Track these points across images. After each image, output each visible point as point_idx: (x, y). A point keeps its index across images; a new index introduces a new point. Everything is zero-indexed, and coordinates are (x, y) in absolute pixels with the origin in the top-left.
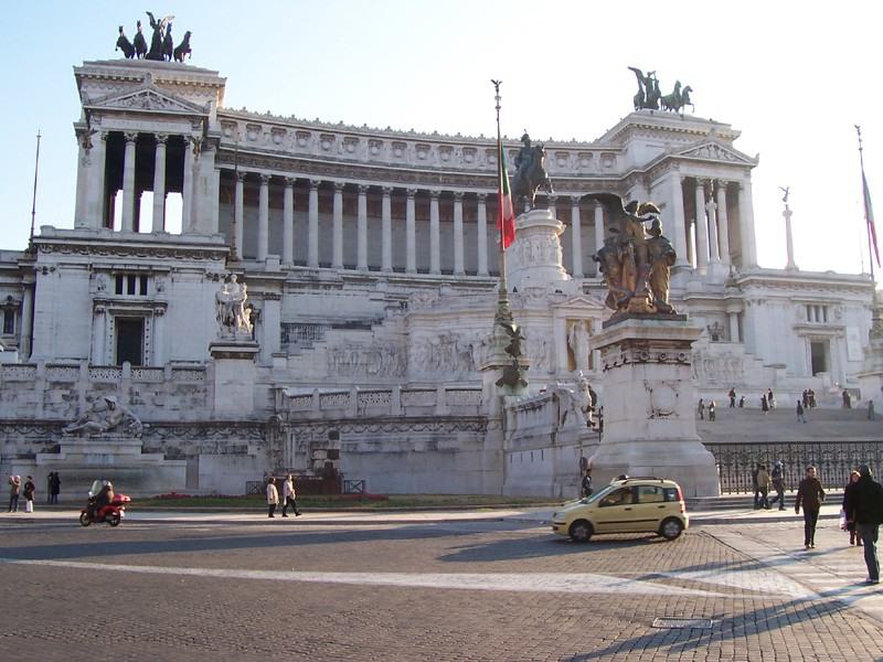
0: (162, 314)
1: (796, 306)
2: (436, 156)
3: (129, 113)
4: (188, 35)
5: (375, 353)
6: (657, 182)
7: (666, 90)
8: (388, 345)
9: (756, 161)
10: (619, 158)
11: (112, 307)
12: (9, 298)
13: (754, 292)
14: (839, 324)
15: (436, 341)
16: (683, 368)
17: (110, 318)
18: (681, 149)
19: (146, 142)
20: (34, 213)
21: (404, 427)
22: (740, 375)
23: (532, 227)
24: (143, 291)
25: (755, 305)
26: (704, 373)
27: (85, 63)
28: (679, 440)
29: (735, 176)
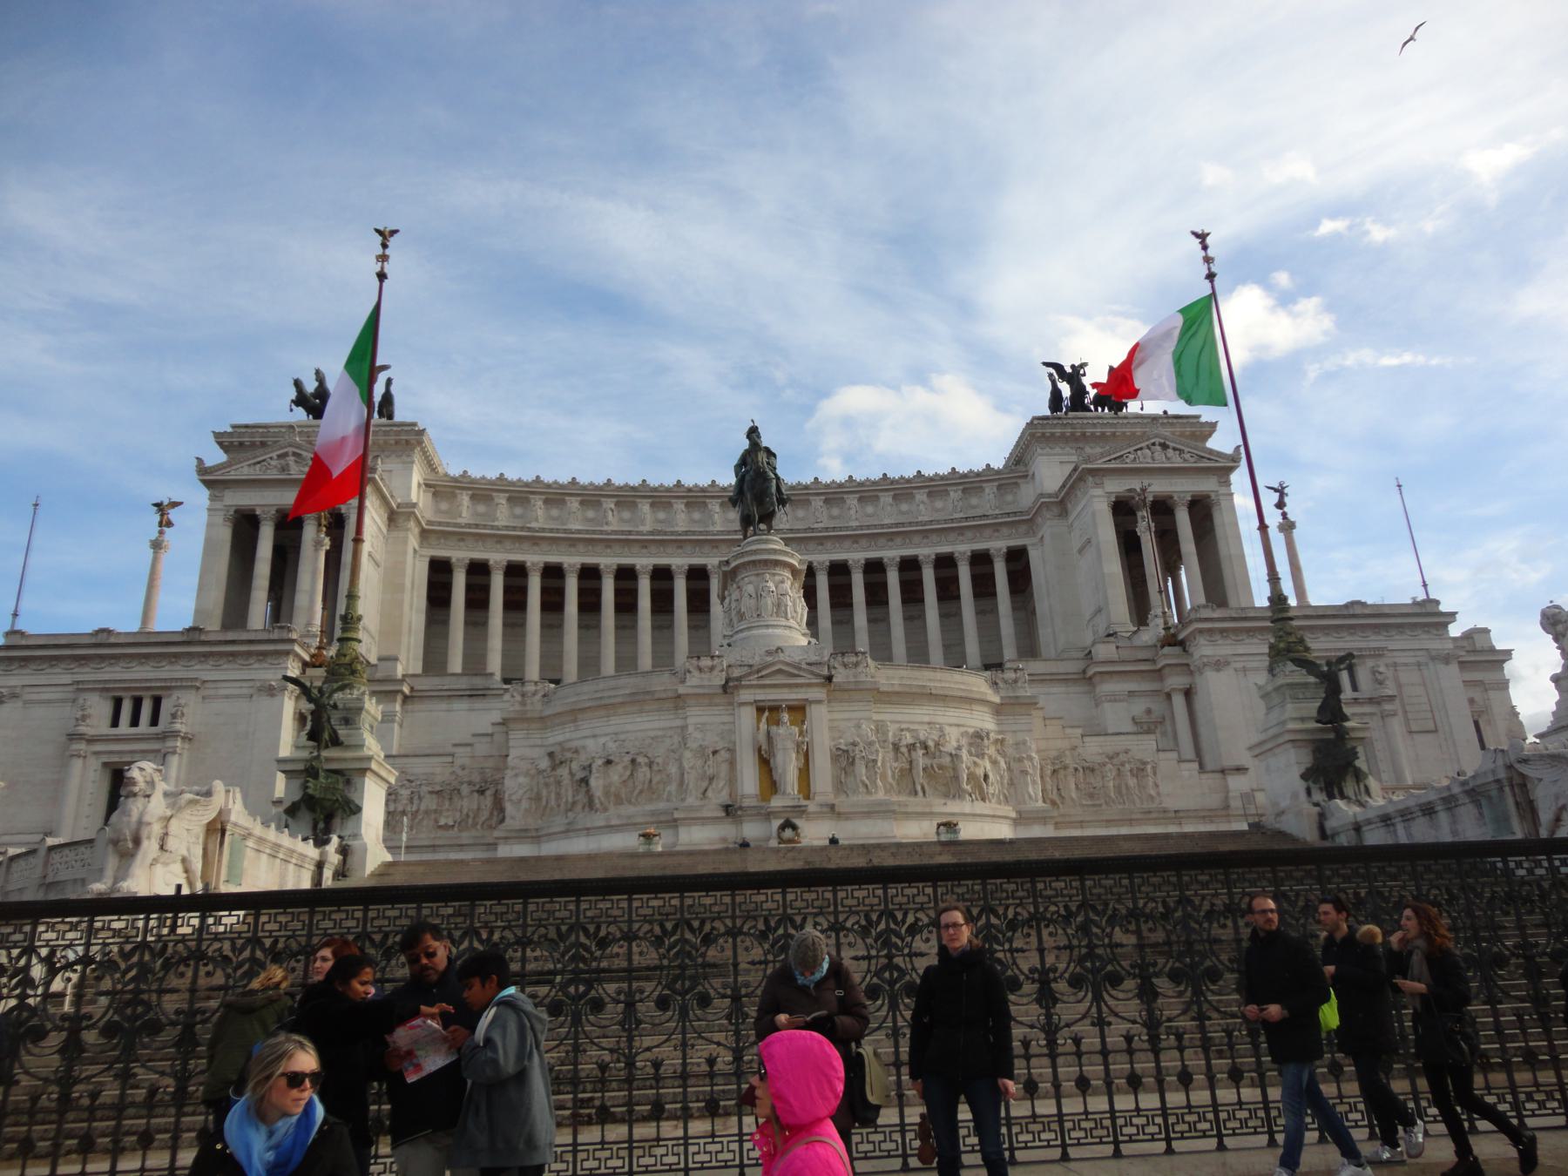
4: (389, 382)
5: (447, 793)
6: (1079, 508)
8: (476, 778)
13: (1204, 649)
15: (545, 764)
18: (1102, 455)
20: (15, 615)
22: (1153, 792)
23: (744, 565)
24: (154, 721)
25: (1210, 675)
26: (1074, 795)
27: (234, 427)
29: (1205, 485)
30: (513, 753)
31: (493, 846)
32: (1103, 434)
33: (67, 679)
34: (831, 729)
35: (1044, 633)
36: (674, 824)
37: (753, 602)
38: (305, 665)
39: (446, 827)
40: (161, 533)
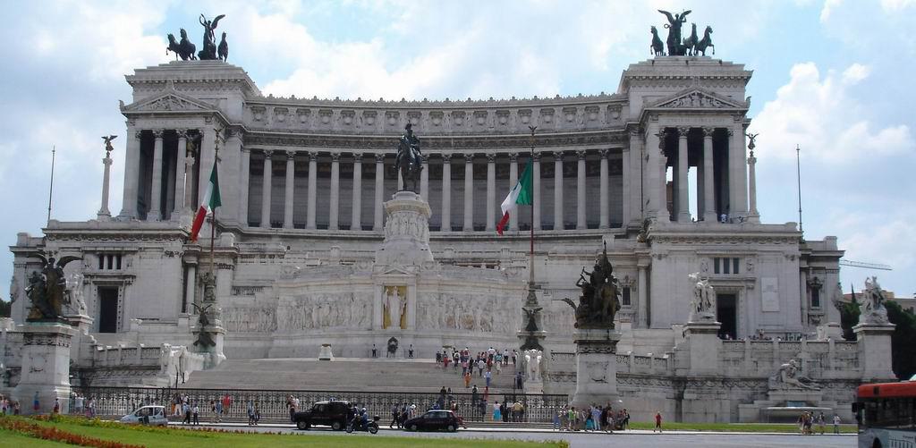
0: (129, 284)
1: (701, 260)
2: (448, 122)
3: (155, 114)
4: (224, 35)
7: (686, 33)
9: (747, 104)
10: (624, 110)
11: (95, 279)
12: (34, 273)
14: (750, 275)
15: (294, 304)
16: (51, 348)
17: (94, 288)
18: (659, 101)
19: (170, 138)
20: (50, 209)
21: (141, 372)
24: (119, 267)
28: (43, 384)
29: (726, 122)
30: (281, 298)
31: (272, 340)
32: (675, 78)
33: (78, 244)
34: (418, 296)
35: (625, 206)
36: (346, 337)
37: (397, 226)
38: (185, 239)
39: (253, 330)
40: (108, 154)
